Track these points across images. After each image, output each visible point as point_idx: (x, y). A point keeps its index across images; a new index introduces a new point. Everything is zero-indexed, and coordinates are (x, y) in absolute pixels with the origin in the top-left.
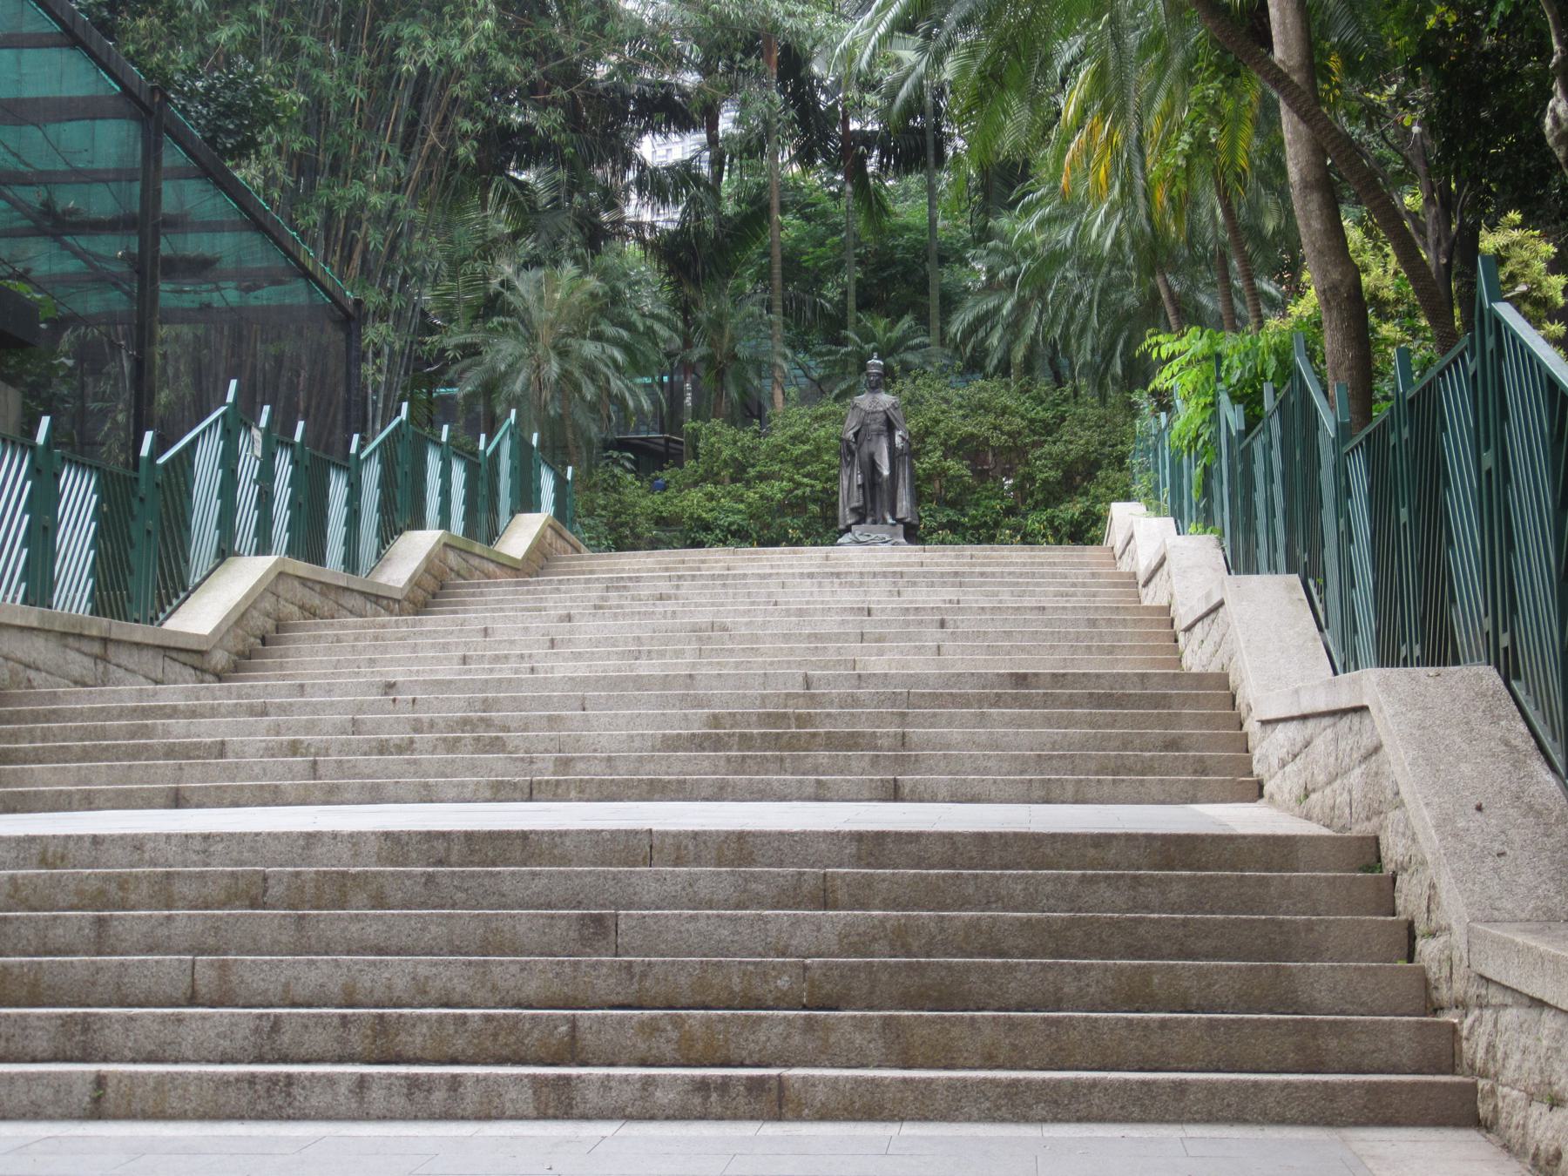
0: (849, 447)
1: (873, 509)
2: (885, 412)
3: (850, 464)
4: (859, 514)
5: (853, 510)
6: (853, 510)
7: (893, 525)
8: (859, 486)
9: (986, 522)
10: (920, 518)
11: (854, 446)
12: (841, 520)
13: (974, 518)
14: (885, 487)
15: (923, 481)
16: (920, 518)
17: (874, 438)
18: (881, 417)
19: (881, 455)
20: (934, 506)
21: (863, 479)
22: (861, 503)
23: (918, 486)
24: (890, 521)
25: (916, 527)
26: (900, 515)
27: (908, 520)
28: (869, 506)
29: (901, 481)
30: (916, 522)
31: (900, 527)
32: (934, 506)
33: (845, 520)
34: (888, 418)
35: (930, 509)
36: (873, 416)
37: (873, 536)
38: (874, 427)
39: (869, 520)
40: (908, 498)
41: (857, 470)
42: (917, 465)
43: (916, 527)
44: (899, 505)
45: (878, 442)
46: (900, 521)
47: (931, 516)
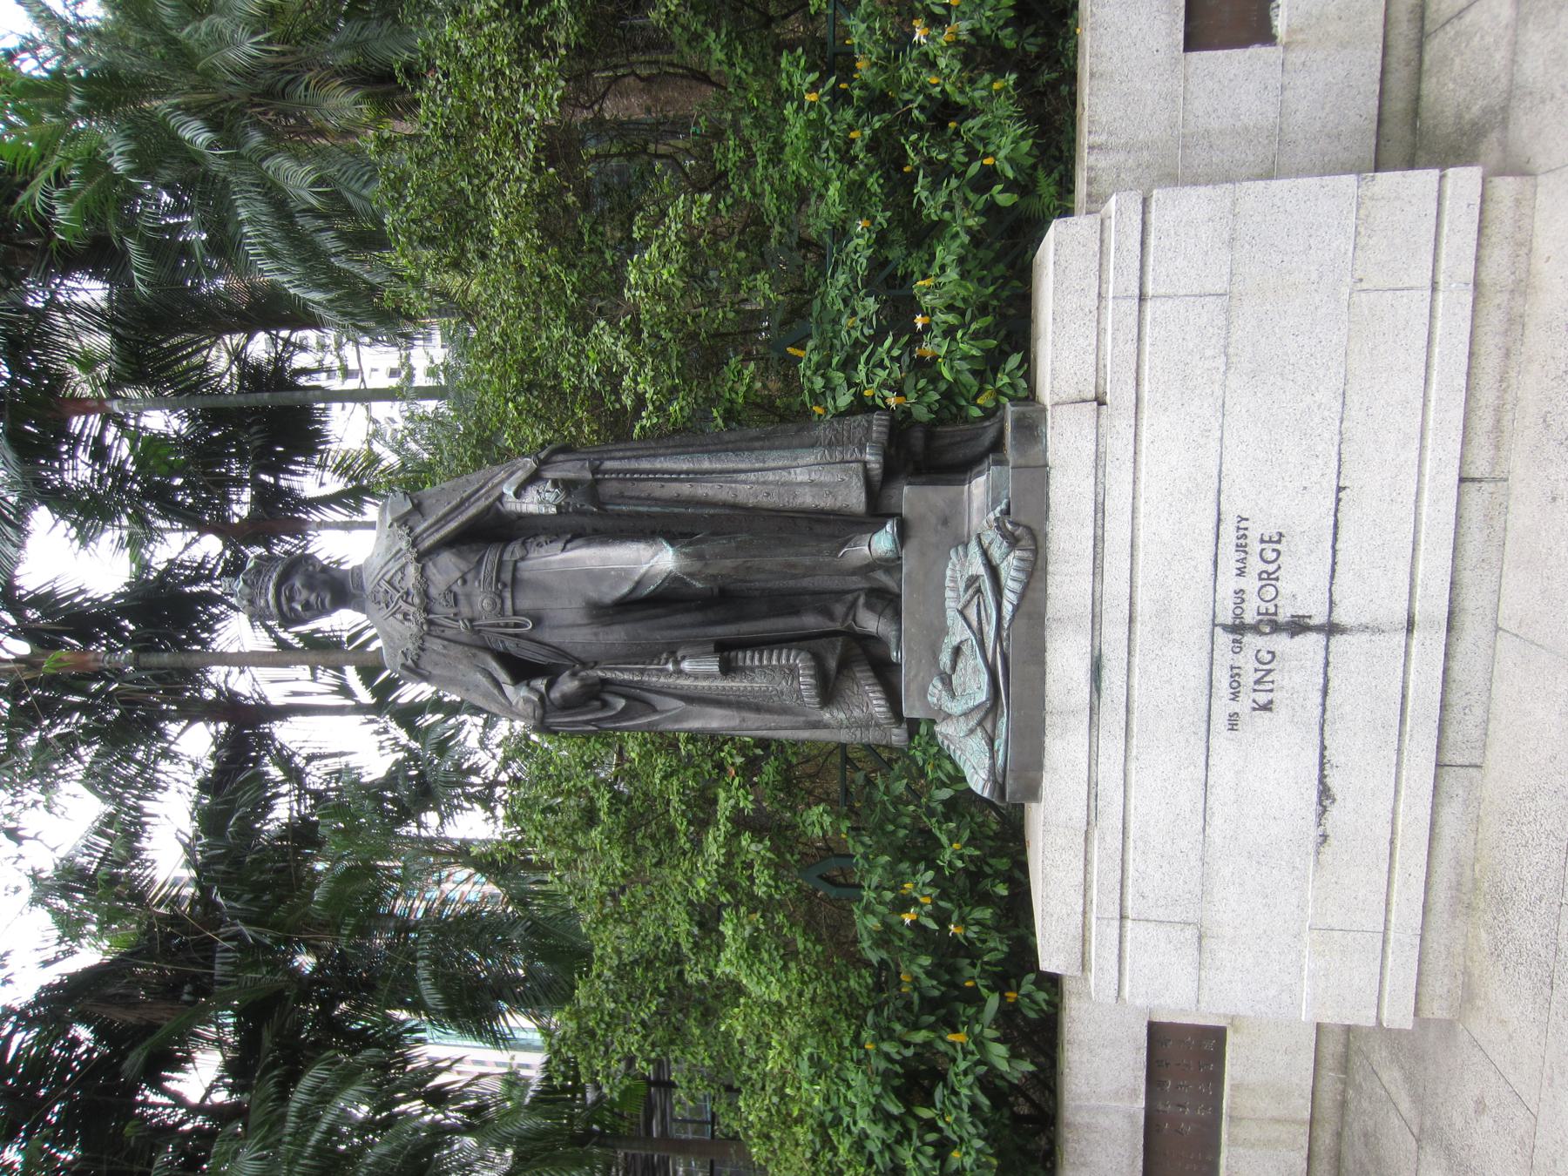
0: (569, 704)
1: (822, 601)
2: (423, 557)
3: (639, 700)
4: (845, 664)
5: (828, 692)
6: (828, 692)
7: (902, 535)
8: (727, 669)
9: (872, 146)
10: (862, 406)
11: (567, 685)
12: (872, 736)
13: (855, 193)
15: (711, 402)
16: (862, 406)
17: (526, 602)
18: (447, 568)
19: (595, 576)
20: (808, 356)
21: (697, 647)
22: (800, 661)
23: (729, 416)
24: (882, 542)
25: (900, 425)
26: (854, 498)
27: (873, 459)
28: (811, 621)
29: (704, 490)
30: (878, 423)
31: (910, 497)
32: (808, 356)
33: (865, 725)
34: (449, 543)
35: (823, 367)
36: (442, 610)
37: (959, 632)
38: (482, 602)
39: (871, 623)
40: (774, 459)
41: (657, 676)
42: (647, 420)
43: (900, 425)
44: (808, 499)
46: (876, 492)
47: (849, 364)
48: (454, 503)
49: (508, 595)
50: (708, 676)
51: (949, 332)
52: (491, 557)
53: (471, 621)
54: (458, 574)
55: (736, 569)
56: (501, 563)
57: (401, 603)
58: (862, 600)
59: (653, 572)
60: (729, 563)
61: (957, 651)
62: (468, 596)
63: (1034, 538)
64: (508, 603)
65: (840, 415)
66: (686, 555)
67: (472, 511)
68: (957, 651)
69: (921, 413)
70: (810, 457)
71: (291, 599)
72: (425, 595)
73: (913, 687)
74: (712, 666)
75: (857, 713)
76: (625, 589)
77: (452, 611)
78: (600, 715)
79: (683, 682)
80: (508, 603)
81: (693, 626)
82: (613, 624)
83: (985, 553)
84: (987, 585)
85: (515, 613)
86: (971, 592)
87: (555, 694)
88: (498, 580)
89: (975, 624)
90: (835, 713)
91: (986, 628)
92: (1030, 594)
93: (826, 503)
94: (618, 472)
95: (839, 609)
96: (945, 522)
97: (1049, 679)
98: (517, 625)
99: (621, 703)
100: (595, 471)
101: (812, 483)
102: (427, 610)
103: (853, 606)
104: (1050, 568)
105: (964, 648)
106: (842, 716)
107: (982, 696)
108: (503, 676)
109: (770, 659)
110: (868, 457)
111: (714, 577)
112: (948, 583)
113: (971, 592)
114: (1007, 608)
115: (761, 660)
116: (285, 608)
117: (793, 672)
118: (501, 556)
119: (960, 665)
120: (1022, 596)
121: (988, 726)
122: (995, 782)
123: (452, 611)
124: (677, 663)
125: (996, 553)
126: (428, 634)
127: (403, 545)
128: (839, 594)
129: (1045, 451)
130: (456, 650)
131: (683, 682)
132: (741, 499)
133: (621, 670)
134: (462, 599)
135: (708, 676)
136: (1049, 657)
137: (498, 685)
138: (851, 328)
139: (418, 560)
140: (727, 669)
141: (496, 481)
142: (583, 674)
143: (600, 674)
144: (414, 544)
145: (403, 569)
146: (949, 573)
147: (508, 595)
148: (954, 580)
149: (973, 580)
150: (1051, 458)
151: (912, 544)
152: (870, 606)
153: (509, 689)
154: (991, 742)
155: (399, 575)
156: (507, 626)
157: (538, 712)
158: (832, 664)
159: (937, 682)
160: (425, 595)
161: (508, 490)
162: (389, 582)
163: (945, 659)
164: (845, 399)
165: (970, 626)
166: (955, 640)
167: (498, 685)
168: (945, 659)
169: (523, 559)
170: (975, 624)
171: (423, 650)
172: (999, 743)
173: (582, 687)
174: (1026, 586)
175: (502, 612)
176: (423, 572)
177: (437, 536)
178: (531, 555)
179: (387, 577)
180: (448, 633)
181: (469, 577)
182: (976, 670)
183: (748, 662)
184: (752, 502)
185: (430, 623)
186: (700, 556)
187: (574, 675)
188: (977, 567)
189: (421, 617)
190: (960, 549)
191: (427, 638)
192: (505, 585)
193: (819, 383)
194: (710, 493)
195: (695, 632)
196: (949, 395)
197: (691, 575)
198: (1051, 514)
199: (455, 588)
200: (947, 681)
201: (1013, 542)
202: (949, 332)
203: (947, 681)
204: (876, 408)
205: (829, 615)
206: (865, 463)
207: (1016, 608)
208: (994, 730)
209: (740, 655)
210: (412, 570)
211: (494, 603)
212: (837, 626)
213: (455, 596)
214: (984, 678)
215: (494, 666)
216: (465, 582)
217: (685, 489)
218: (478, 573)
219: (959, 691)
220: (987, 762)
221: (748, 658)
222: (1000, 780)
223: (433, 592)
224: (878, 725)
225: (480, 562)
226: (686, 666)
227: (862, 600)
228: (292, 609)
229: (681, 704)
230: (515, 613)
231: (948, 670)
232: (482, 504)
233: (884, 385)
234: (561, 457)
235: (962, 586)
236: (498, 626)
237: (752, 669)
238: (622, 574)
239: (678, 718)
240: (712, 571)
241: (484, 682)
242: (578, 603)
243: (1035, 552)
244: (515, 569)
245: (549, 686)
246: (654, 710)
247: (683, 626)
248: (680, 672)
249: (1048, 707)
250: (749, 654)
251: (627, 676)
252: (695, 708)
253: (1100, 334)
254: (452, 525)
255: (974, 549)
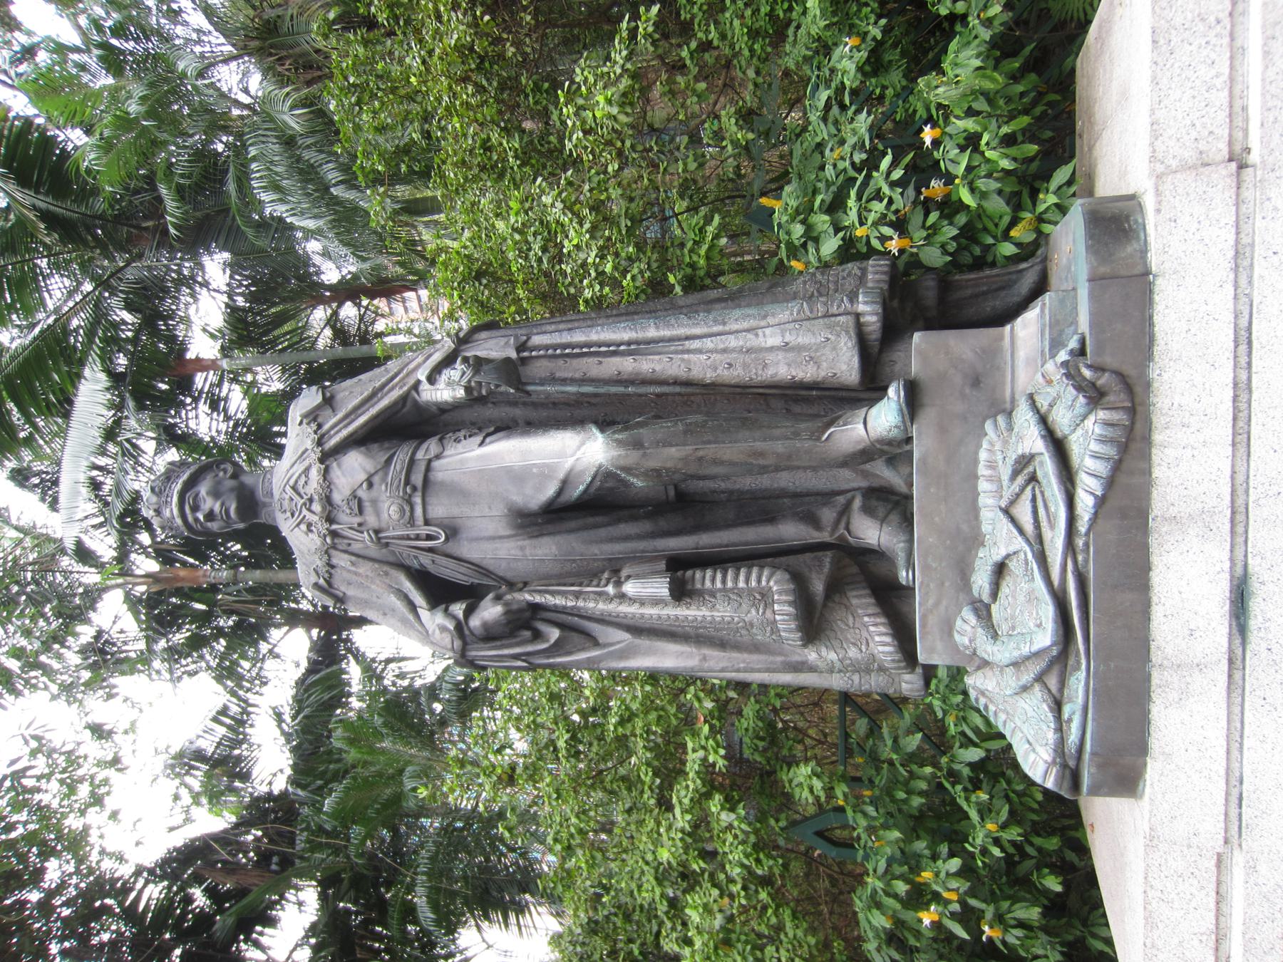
4: (835, 588)
8: (681, 592)
10: (850, 251)
11: (490, 611)
12: (874, 683)
14: (671, 456)
16: (850, 251)
17: (439, 510)
18: (354, 467)
19: (518, 476)
22: (775, 583)
27: (869, 311)
28: (791, 531)
29: (649, 365)
30: (875, 272)
32: (783, 205)
36: (346, 520)
38: (388, 510)
39: (870, 532)
40: (738, 319)
44: (782, 370)
45: (457, 491)
47: (836, 206)
48: (366, 394)
49: (418, 500)
50: (656, 602)
51: (971, 141)
52: (402, 456)
53: (377, 532)
54: (363, 477)
55: (685, 460)
56: (412, 462)
57: (305, 512)
58: (857, 503)
59: (579, 468)
60: (673, 451)
61: (1000, 569)
62: (374, 502)
63: (1129, 388)
64: (419, 511)
65: (825, 266)
66: (619, 442)
67: (385, 402)
68: (1000, 569)
69: (934, 257)
70: (784, 313)
71: (195, 509)
72: (328, 500)
73: (933, 620)
74: (660, 587)
75: (853, 653)
76: (550, 491)
77: (356, 520)
78: (530, 648)
79: (625, 609)
80: (419, 511)
81: (640, 537)
82: (542, 535)
83: (1043, 420)
84: (1047, 468)
85: (427, 523)
86: (1020, 480)
87: (475, 622)
88: (407, 482)
89: (1029, 527)
90: (824, 651)
91: (1047, 534)
92: (1122, 479)
93: (807, 373)
94: (547, 348)
95: (828, 515)
96: (976, 382)
97: (1157, 613)
98: (429, 537)
99: (554, 634)
100: (521, 348)
101: (786, 347)
102: (330, 519)
103: (846, 510)
104: (1157, 437)
105: (1013, 565)
106: (832, 656)
107: (1045, 638)
108: (419, 600)
109: (736, 579)
110: (861, 308)
111: (657, 472)
112: (982, 470)
113: (1020, 480)
114: (1085, 504)
115: (724, 581)
116: (190, 519)
117: (764, 597)
118: (414, 454)
119: (1005, 590)
120: (1110, 483)
121: (1053, 682)
122: (1064, 766)
123: (356, 520)
124: (619, 584)
125: (1062, 419)
126: (334, 547)
127: (309, 444)
128: (827, 496)
129: (1144, 251)
130: (365, 568)
131: (625, 609)
132: (697, 373)
133: (553, 593)
134: (367, 504)
135: (656, 602)
136: (1159, 578)
137: (413, 607)
138: (839, 159)
139: (321, 461)
140: (681, 592)
141: (411, 366)
142: (508, 597)
143: (528, 597)
144: (320, 443)
145: (307, 471)
146: (983, 455)
147: (418, 500)
148: (992, 465)
149: (1025, 461)
150: (1155, 260)
151: (928, 416)
152: (868, 510)
153: (424, 614)
154: (1057, 706)
155: (303, 479)
156: (418, 538)
157: (458, 643)
158: (818, 586)
159: (967, 613)
160: (328, 500)
161: (422, 375)
162: (294, 488)
163: (981, 581)
164: (830, 245)
165: (1021, 531)
166: (998, 554)
167: (413, 607)
168: (981, 581)
169: (438, 457)
170: (1029, 527)
171: (333, 567)
172: (1072, 709)
173: (507, 613)
174: (1117, 467)
175: (412, 522)
176: (326, 473)
177: (345, 433)
178: (446, 453)
179: (292, 482)
180: (356, 547)
181: (376, 479)
182: (1031, 598)
183: (708, 584)
184: (709, 376)
185: (334, 534)
186: (637, 445)
187: (498, 598)
188: (1032, 441)
189: (322, 527)
190: (1001, 419)
191: (333, 552)
192: (414, 489)
193: (798, 230)
194: (658, 368)
195: (642, 545)
196: (969, 234)
197: (627, 470)
198: (1158, 350)
199: (361, 493)
200: (983, 612)
201: (1095, 396)
202: (971, 141)
203: (983, 612)
204: (872, 252)
205: (812, 520)
206: (858, 316)
207: (1101, 502)
208: (1061, 690)
209: (698, 574)
210: (315, 474)
211: (402, 511)
212: (825, 536)
213: (360, 502)
214: (1048, 611)
215: (408, 586)
216: (370, 485)
217: (627, 365)
218: (386, 474)
219: (1003, 629)
220: (1051, 736)
221: (707, 579)
222: (1072, 763)
223: (337, 497)
224: (882, 669)
225: (388, 462)
226: (630, 588)
227: (857, 503)
228: (197, 520)
229: (626, 636)
230: (427, 523)
231: (986, 598)
232: (396, 394)
233: (882, 220)
234: (484, 335)
235: (1006, 472)
236: (408, 538)
237: (713, 594)
238: (545, 473)
239: (624, 654)
240: (653, 463)
241: (399, 605)
242: (499, 510)
243: (1132, 411)
244: (428, 469)
245: (469, 612)
246: (596, 643)
247: (627, 538)
248: (622, 597)
249: (1156, 657)
250: (709, 573)
251: (558, 601)
252: (644, 642)
253: (1236, 53)
254: (362, 420)
255: (1024, 416)
